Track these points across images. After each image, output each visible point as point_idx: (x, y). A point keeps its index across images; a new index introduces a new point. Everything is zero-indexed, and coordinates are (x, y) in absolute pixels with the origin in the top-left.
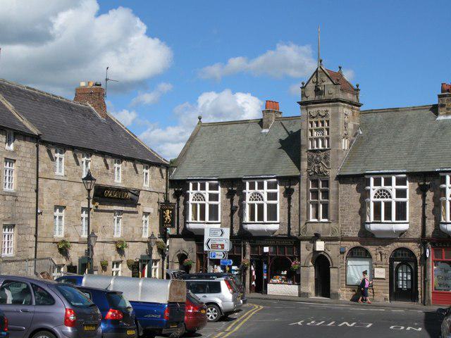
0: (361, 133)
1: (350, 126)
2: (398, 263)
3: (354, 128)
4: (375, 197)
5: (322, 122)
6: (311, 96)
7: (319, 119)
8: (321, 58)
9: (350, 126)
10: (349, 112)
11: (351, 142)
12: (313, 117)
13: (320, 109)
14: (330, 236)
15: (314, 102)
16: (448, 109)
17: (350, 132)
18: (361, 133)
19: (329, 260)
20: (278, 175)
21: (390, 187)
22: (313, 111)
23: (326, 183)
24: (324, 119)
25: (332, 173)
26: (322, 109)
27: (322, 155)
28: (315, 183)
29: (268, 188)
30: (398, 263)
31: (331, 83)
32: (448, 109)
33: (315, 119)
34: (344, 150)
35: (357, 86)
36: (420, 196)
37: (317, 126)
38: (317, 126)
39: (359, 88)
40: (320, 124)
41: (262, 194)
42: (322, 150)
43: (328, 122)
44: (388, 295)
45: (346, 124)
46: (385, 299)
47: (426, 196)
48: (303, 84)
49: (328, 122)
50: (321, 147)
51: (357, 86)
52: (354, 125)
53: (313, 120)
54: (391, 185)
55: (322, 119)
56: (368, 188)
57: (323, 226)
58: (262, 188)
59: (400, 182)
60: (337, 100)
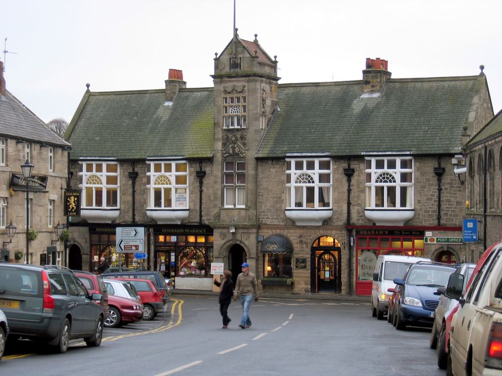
0: (279, 109)
1: (268, 102)
2: (322, 252)
3: (272, 105)
4: (296, 182)
5: (238, 99)
6: (227, 70)
7: (235, 95)
8: (236, 27)
9: (268, 102)
10: (267, 87)
11: (269, 121)
12: (229, 93)
13: (236, 84)
14: (246, 223)
15: (230, 76)
16: (373, 86)
17: (268, 110)
18: (279, 109)
19: (246, 249)
20: (120, 158)
21: (170, 173)
22: (229, 85)
23: (242, 166)
24: (240, 95)
25: (251, 154)
26: (239, 83)
27: (239, 135)
28: (229, 165)
29: (107, 171)
30: (322, 252)
31: (249, 56)
32: (373, 86)
33: (231, 96)
34: (262, 129)
35: (275, 57)
36: (130, 182)
37: (232, 102)
38: (232, 102)
39: (277, 60)
40: (236, 100)
41: (101, 177)
42: (237, 130)
43: (245, 98)
44: (309, 287)
45: (264, 100)
46: (306, 291)
47: (351, 180)
48: (216, 54)
49: (245, 98)
50: (236, 127)
51: (275, 57)
52: (272, 101)
53: (228, 96)
54: (314, 169)
55: (238, 95)
56: (80, 173)
57: (239, 212)
58: (101, 171)
59: (404, 165)
60: (255, 75)
